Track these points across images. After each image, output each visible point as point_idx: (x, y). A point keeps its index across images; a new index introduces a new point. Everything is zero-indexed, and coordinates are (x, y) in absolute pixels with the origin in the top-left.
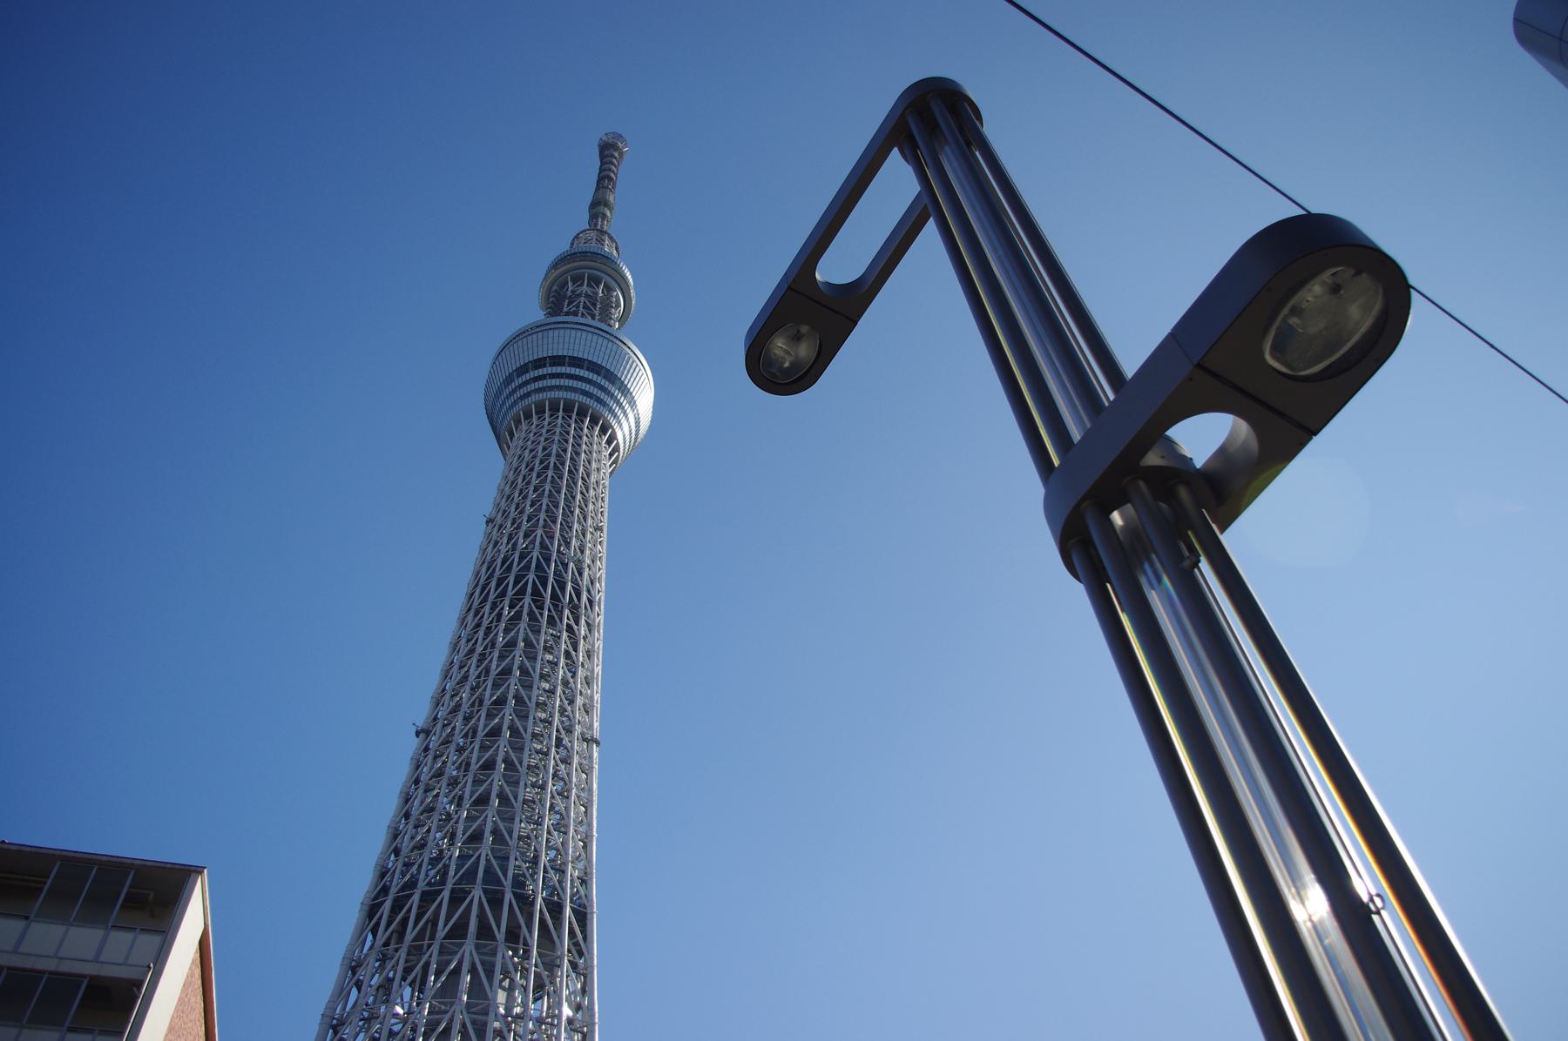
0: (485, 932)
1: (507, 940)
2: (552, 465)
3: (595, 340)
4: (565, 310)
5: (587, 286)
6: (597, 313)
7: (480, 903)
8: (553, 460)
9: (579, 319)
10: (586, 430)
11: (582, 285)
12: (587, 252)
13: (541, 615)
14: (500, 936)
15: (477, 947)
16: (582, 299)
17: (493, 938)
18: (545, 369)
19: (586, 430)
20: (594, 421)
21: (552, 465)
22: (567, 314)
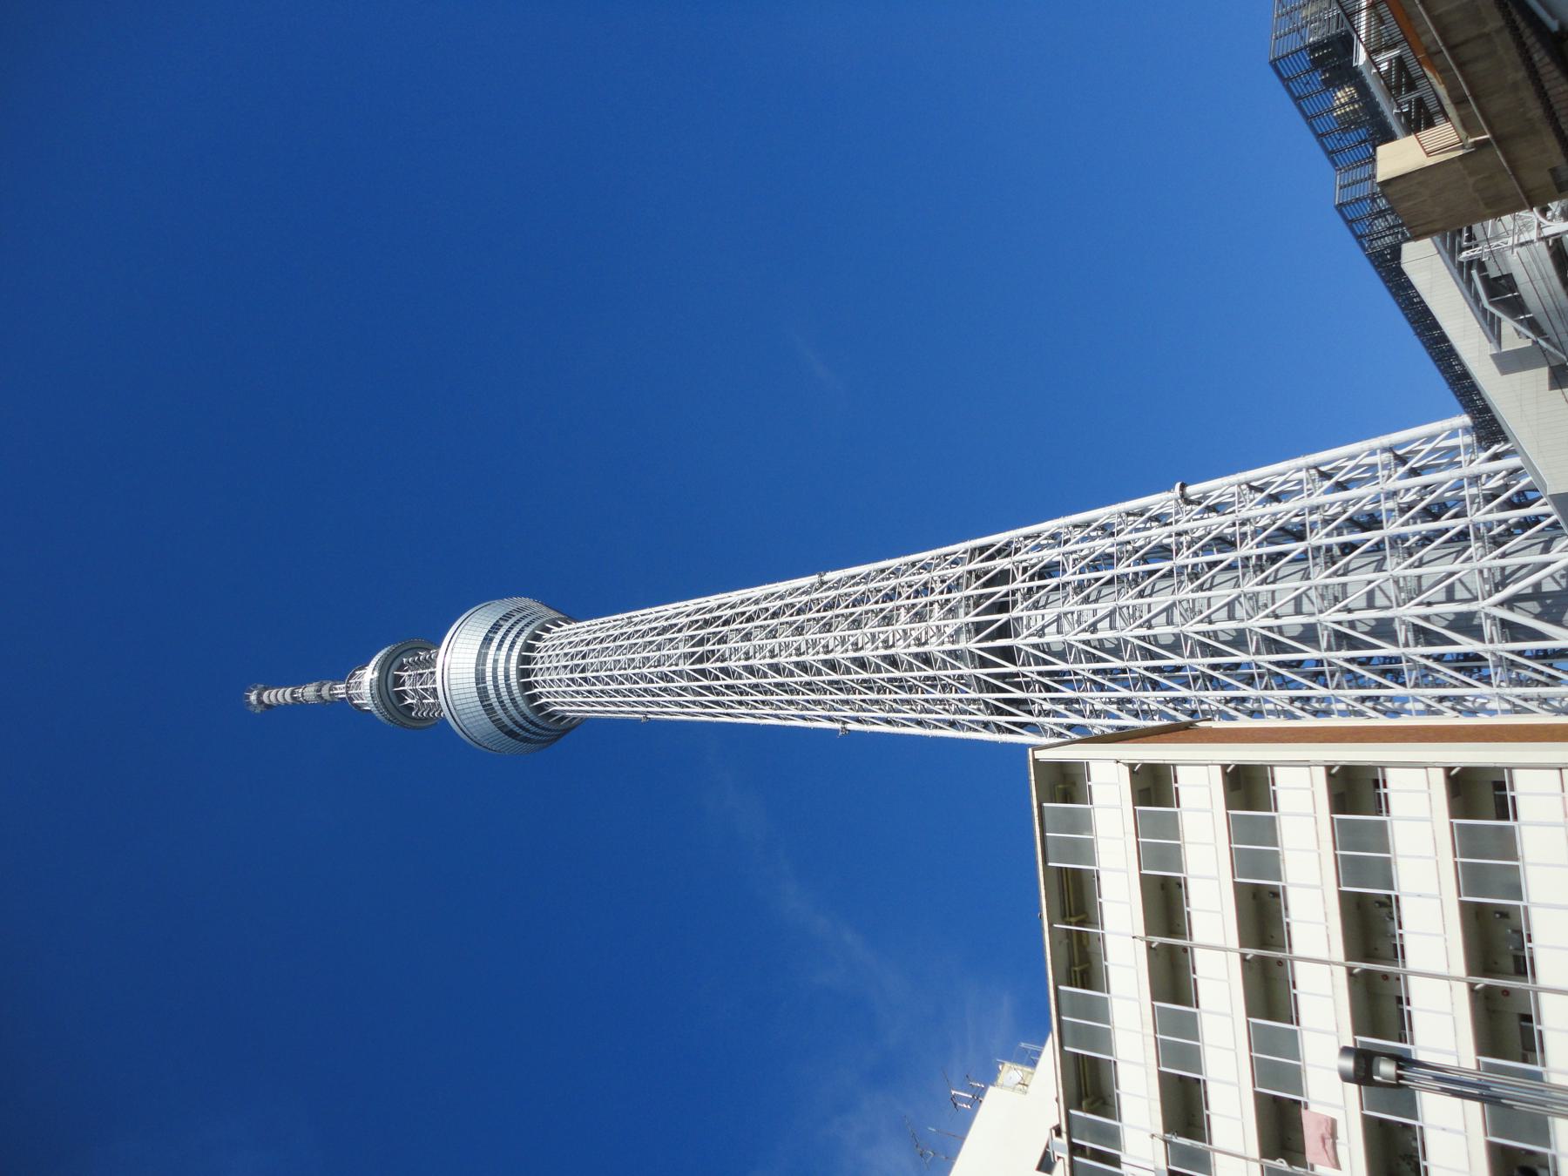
0: (1004, 631)
1: (1007, 611)
2: (581, 675)
3: (460, 645)
4: (432, 701)
5: (404, 686)
6: (427, 671)
7: (979, 641)
8: (576, 675)
9: (439, 686)
10: (546, 644)
11: (404, 691)
12: (372, 694)
13: (719, 651)
14: (1004, 617)
15: (1017, 635)
16: (418, 687)
17: (1007, 623)
18: (488, 688)
19: (546, 644)
20: (538, 638)
21: (581, 675)
22: (436, 697)
